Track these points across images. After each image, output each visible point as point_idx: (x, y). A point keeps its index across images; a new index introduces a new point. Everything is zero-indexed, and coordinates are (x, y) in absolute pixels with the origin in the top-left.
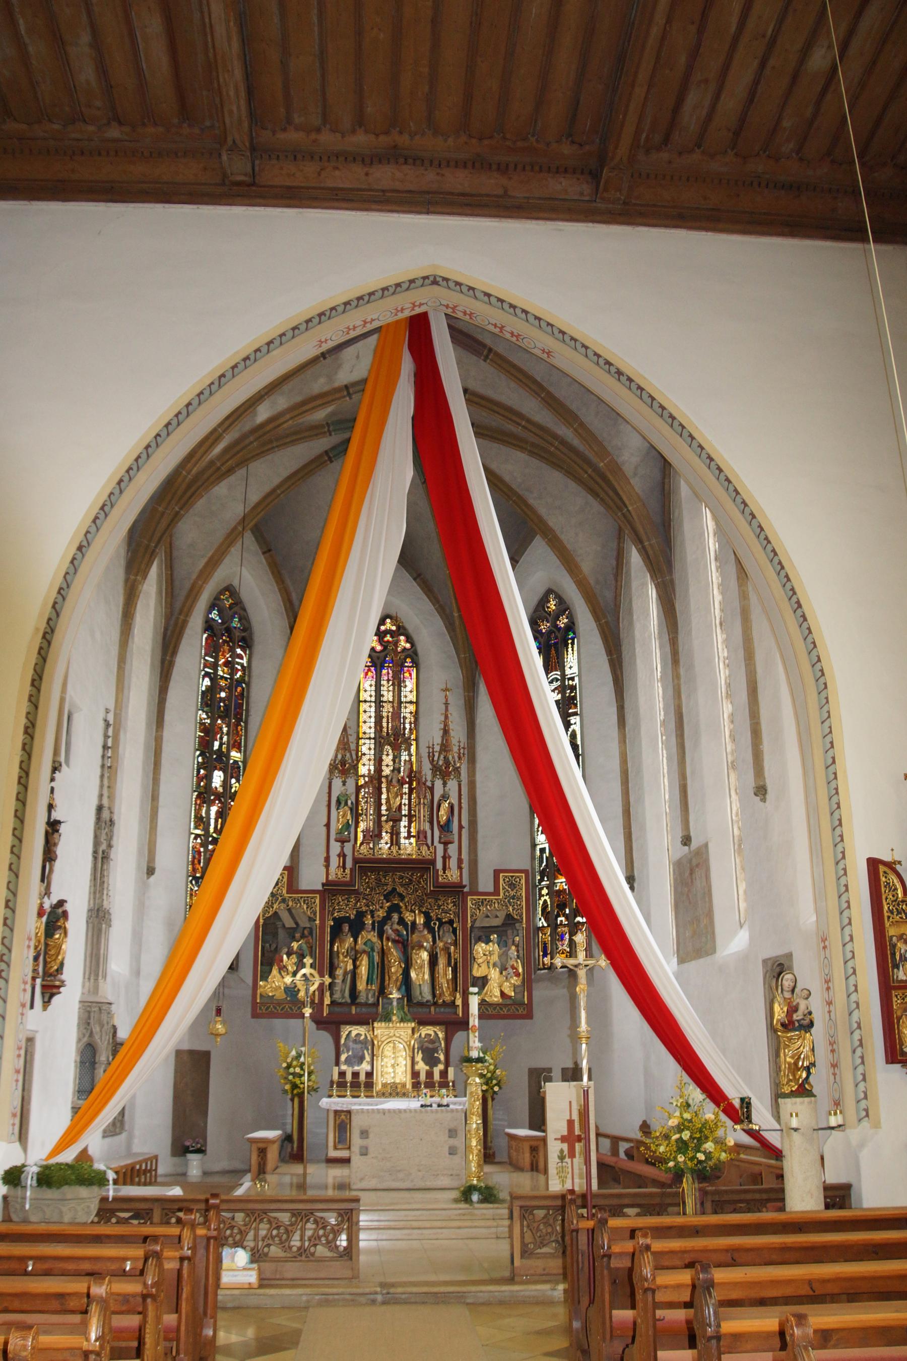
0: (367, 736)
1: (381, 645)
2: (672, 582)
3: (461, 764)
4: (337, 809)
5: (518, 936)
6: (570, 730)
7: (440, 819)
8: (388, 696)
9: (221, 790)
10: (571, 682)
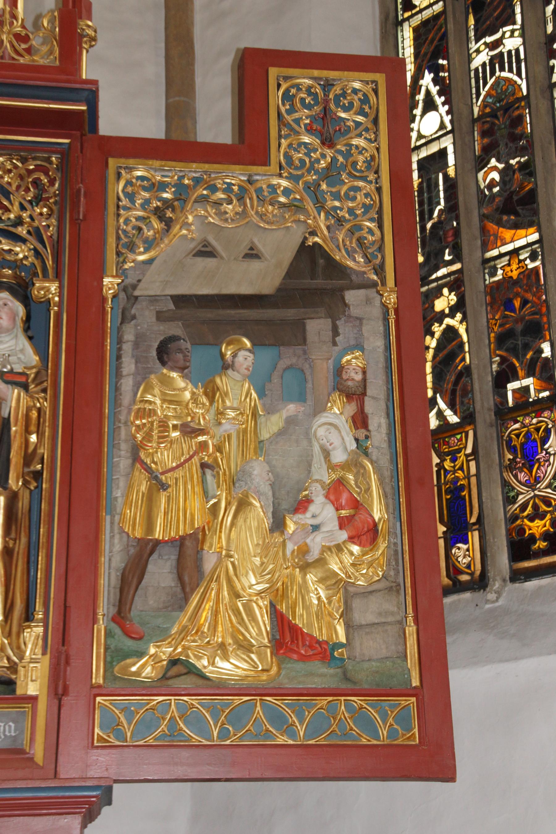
5: (360, 347)
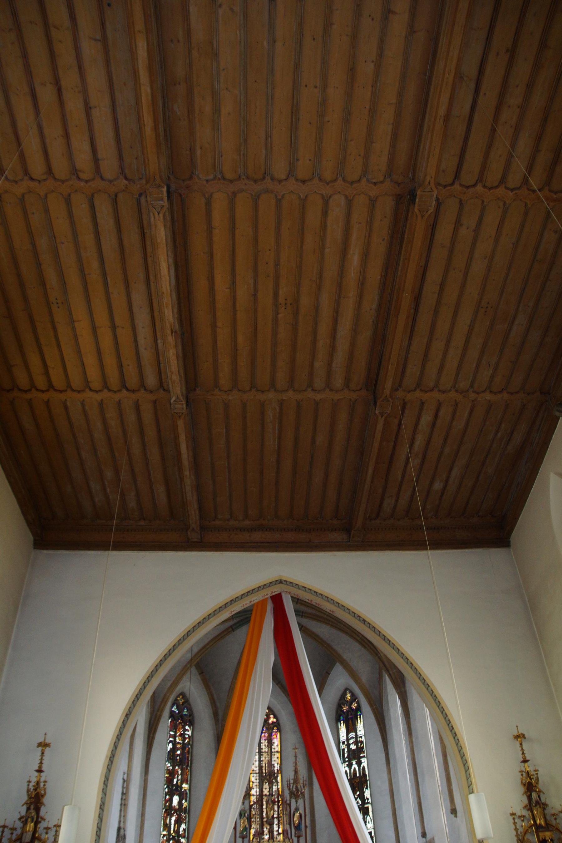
0: (255, 772)
2: (405, 692)
3: (305, 790)
4: (240, 819)
6: (362, 766)
7: (295, 822)
8: (265, 749)
9: (177, 807)
10: (360, 739)
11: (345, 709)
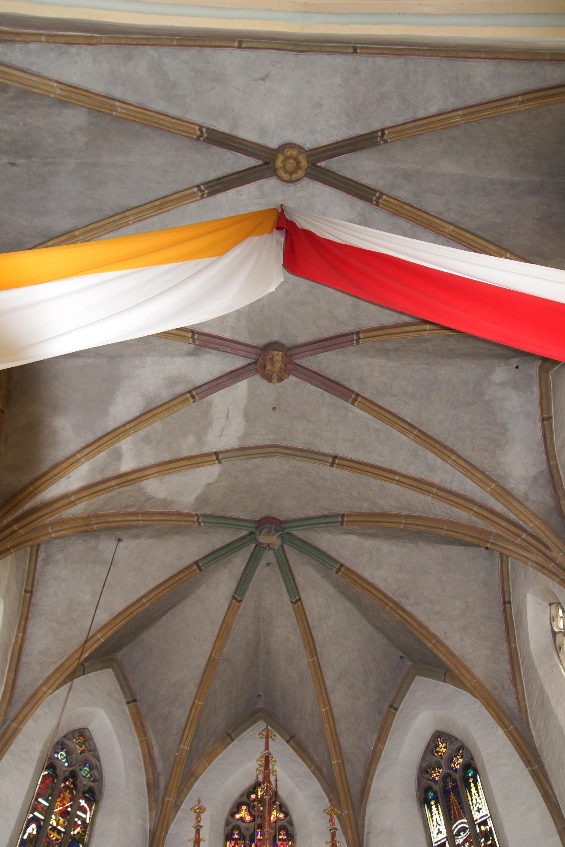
1: (251, 814)
11: (436, 776)
